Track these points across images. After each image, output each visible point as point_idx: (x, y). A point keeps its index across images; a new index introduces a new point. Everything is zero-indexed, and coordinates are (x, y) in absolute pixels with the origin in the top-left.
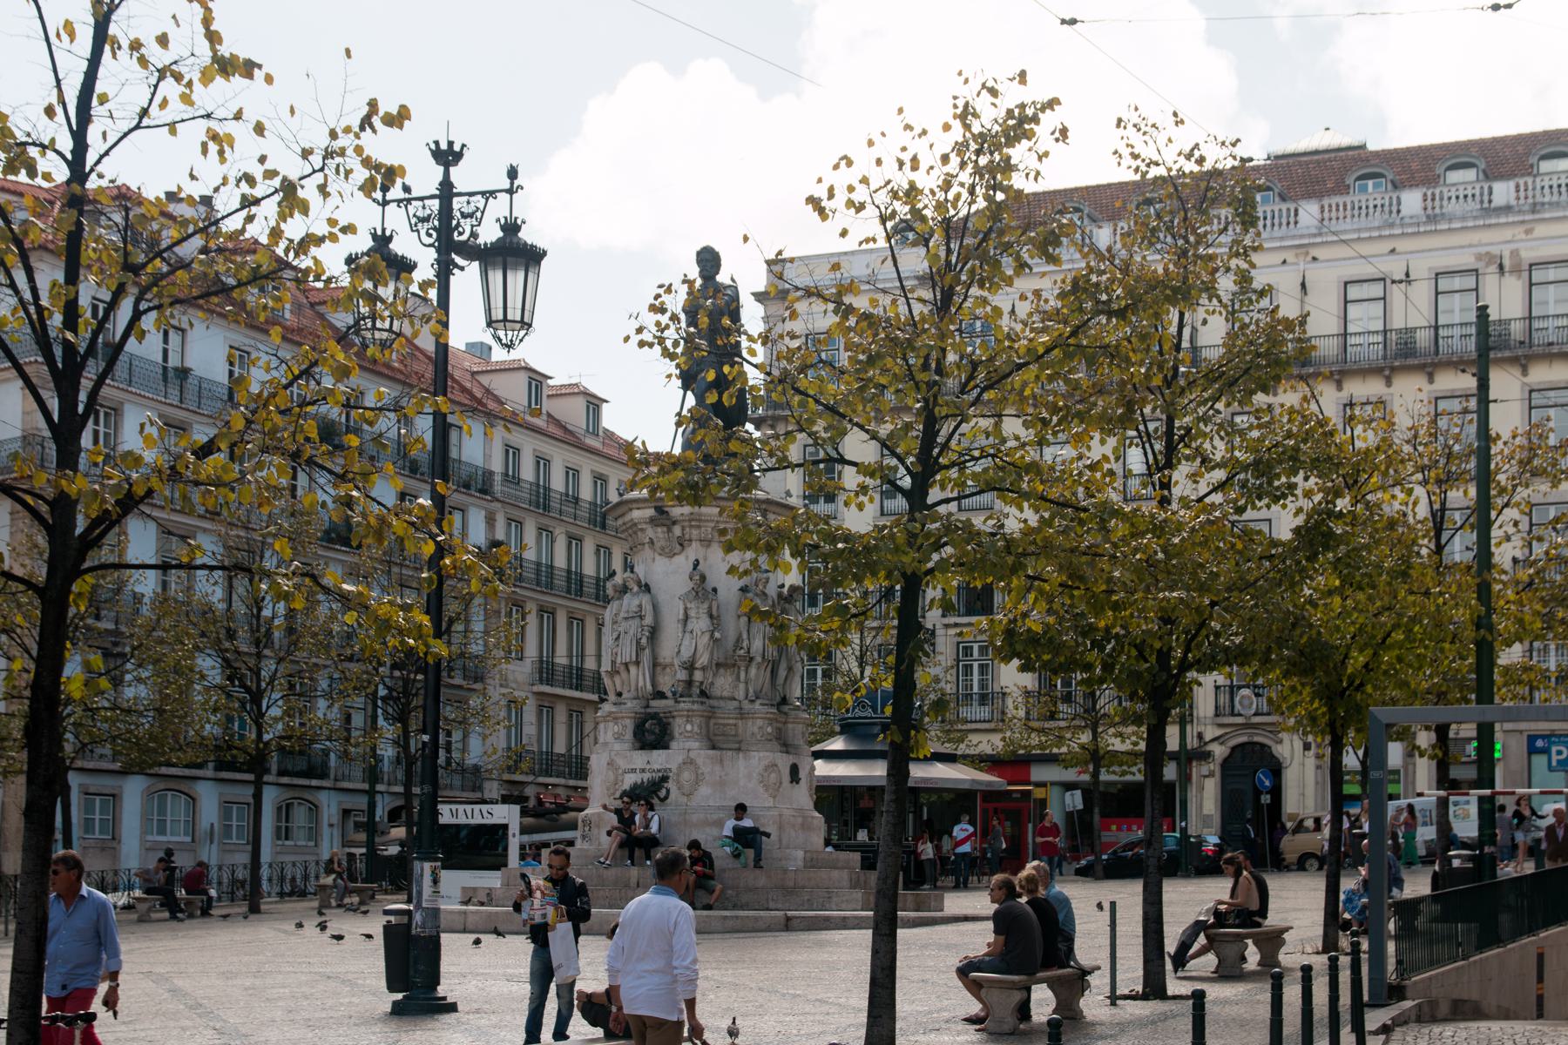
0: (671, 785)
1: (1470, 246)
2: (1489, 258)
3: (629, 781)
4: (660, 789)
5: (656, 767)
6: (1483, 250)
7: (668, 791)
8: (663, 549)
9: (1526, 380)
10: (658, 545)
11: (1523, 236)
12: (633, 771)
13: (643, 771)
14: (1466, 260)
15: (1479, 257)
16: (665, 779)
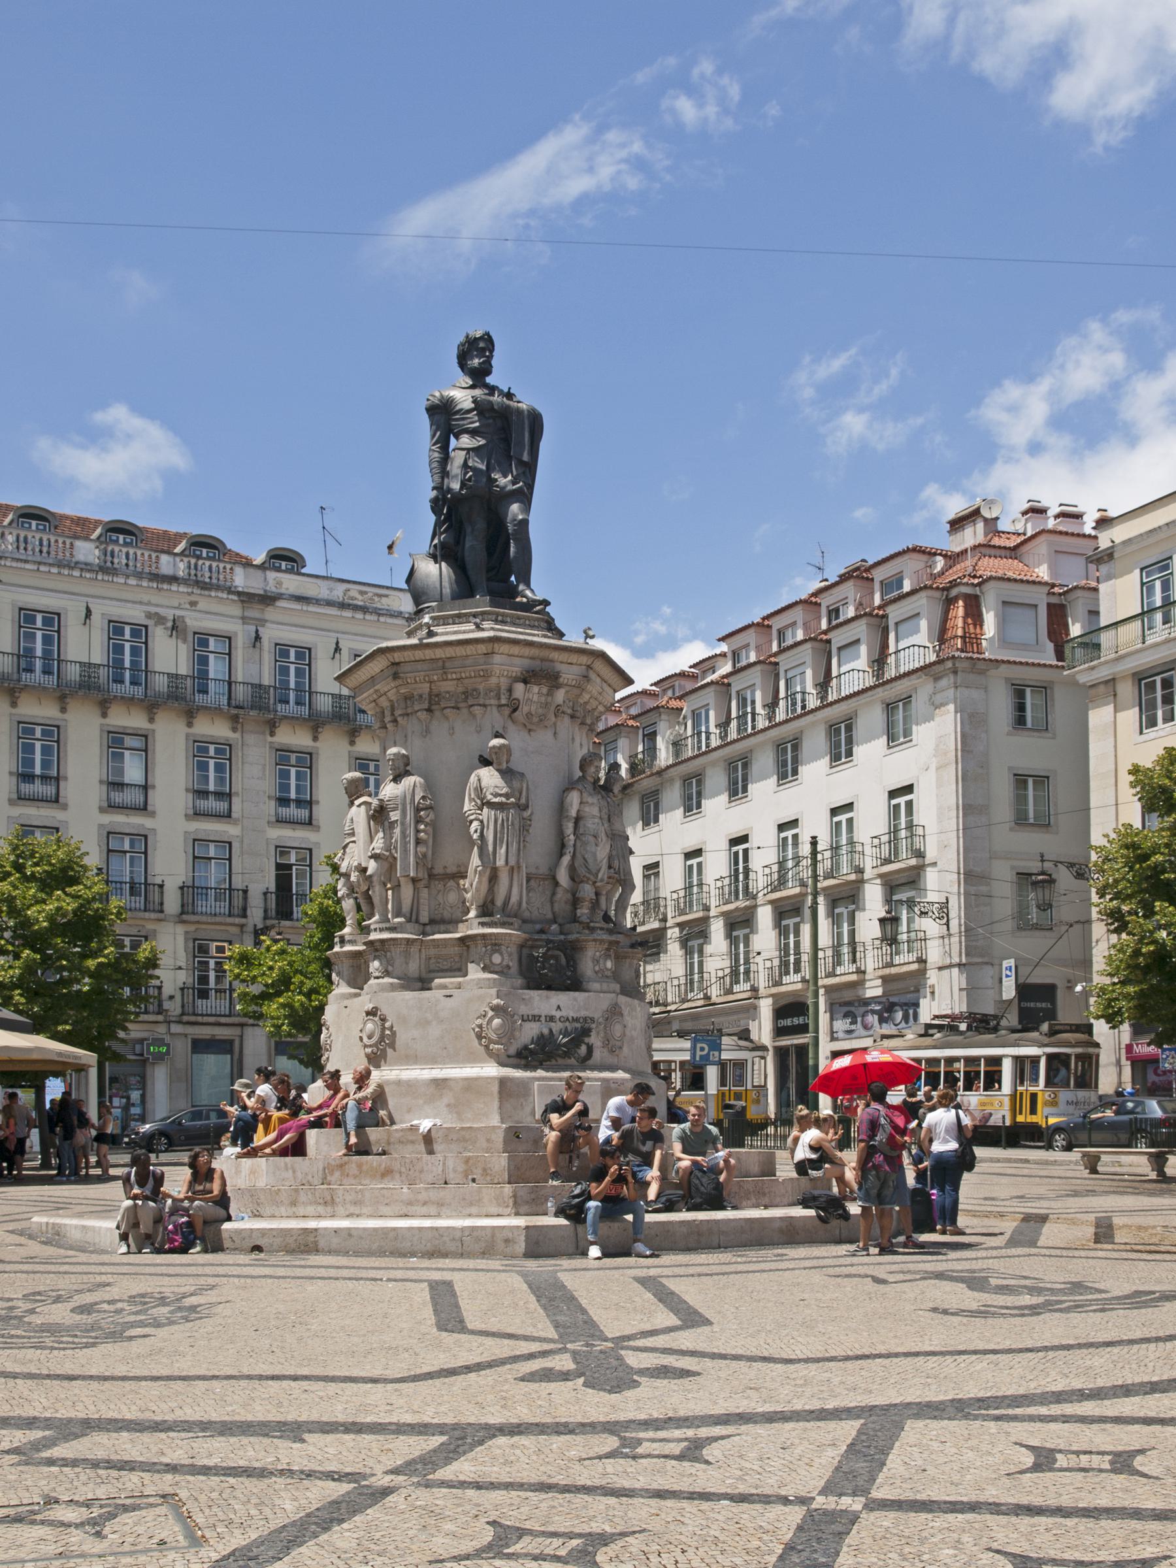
0: (595, 1039)
1: (141, 603)
2: (160, 620)
3: (529, 1032)
4: (578, 1046)
5: (571, 1014)
6: (153, 610)
7: (590, 1049)
8: (529, 715)
9: (191, 731)
10: (524, 709)
11: (188, 606)
12: (536, 1018)
13: (551, 1019)
14: (135, 614)
15: (149, 616)
16: (586, 1032)
